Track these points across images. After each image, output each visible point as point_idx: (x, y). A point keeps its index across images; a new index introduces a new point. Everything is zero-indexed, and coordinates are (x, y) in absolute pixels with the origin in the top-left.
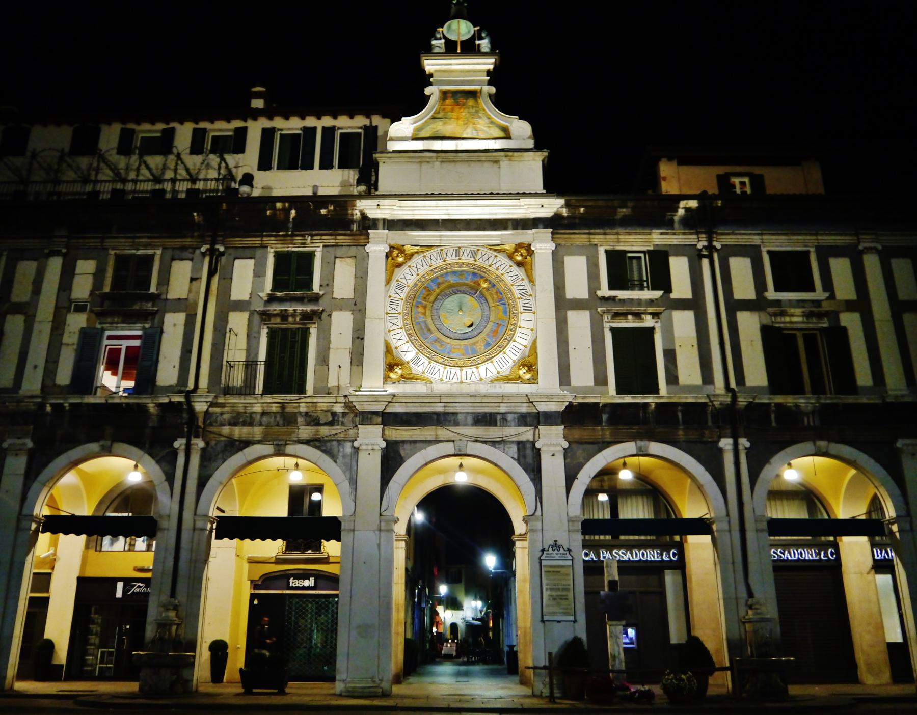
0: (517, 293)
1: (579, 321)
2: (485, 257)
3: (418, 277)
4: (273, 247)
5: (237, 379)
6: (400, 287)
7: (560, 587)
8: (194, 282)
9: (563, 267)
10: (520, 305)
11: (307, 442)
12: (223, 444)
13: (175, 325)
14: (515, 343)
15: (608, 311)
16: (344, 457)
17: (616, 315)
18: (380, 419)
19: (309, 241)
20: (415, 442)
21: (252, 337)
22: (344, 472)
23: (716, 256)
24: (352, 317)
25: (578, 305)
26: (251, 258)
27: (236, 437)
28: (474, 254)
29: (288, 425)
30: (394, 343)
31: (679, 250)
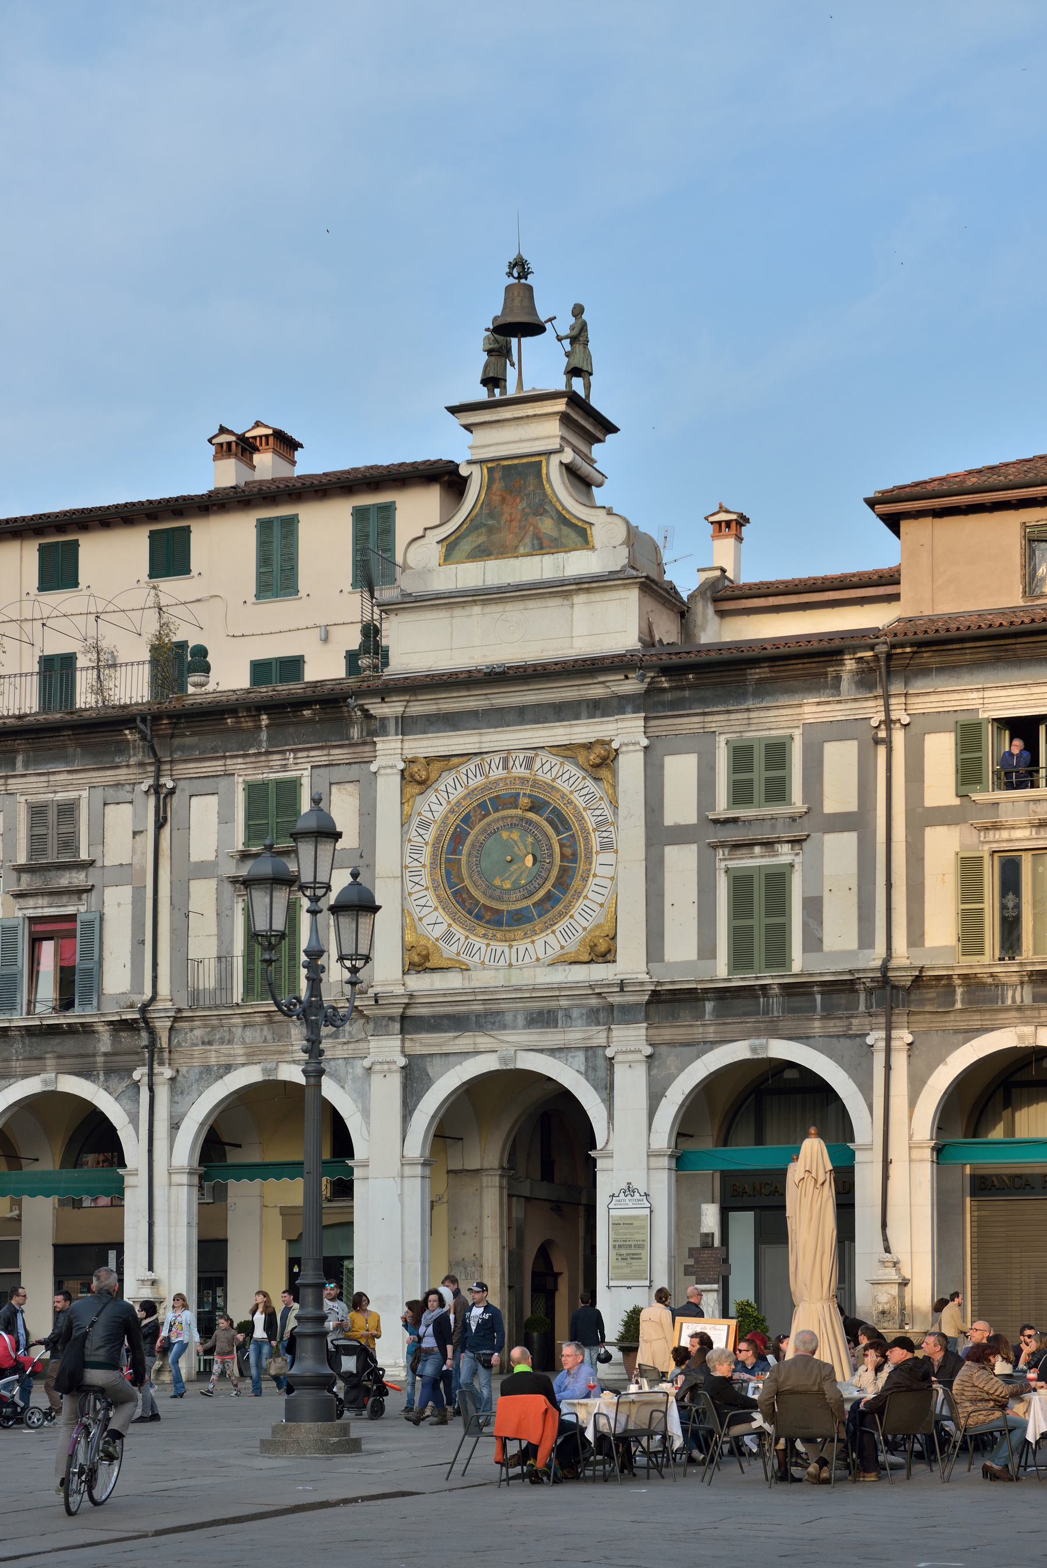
0: (590, 821)
1: (682, 862)
2: (547, 767)
4: (244, 773)
5: (208, 979)
6: (425, 825)
7: (633, 1243)
8: (137, 837)
9: (663, 775)
10: (595, 840)
14: (586, 902)
15: (722, 845)
16: (354, 1080)
18: (397, 1026)
19: (291, 761)
21: (223, 916)
22: (355, 1101)
25: (681, 835)
26: (213, 794)
27: (213, 1061)
28: (529, 763)
30: (417, 912)
31: (840, 731)
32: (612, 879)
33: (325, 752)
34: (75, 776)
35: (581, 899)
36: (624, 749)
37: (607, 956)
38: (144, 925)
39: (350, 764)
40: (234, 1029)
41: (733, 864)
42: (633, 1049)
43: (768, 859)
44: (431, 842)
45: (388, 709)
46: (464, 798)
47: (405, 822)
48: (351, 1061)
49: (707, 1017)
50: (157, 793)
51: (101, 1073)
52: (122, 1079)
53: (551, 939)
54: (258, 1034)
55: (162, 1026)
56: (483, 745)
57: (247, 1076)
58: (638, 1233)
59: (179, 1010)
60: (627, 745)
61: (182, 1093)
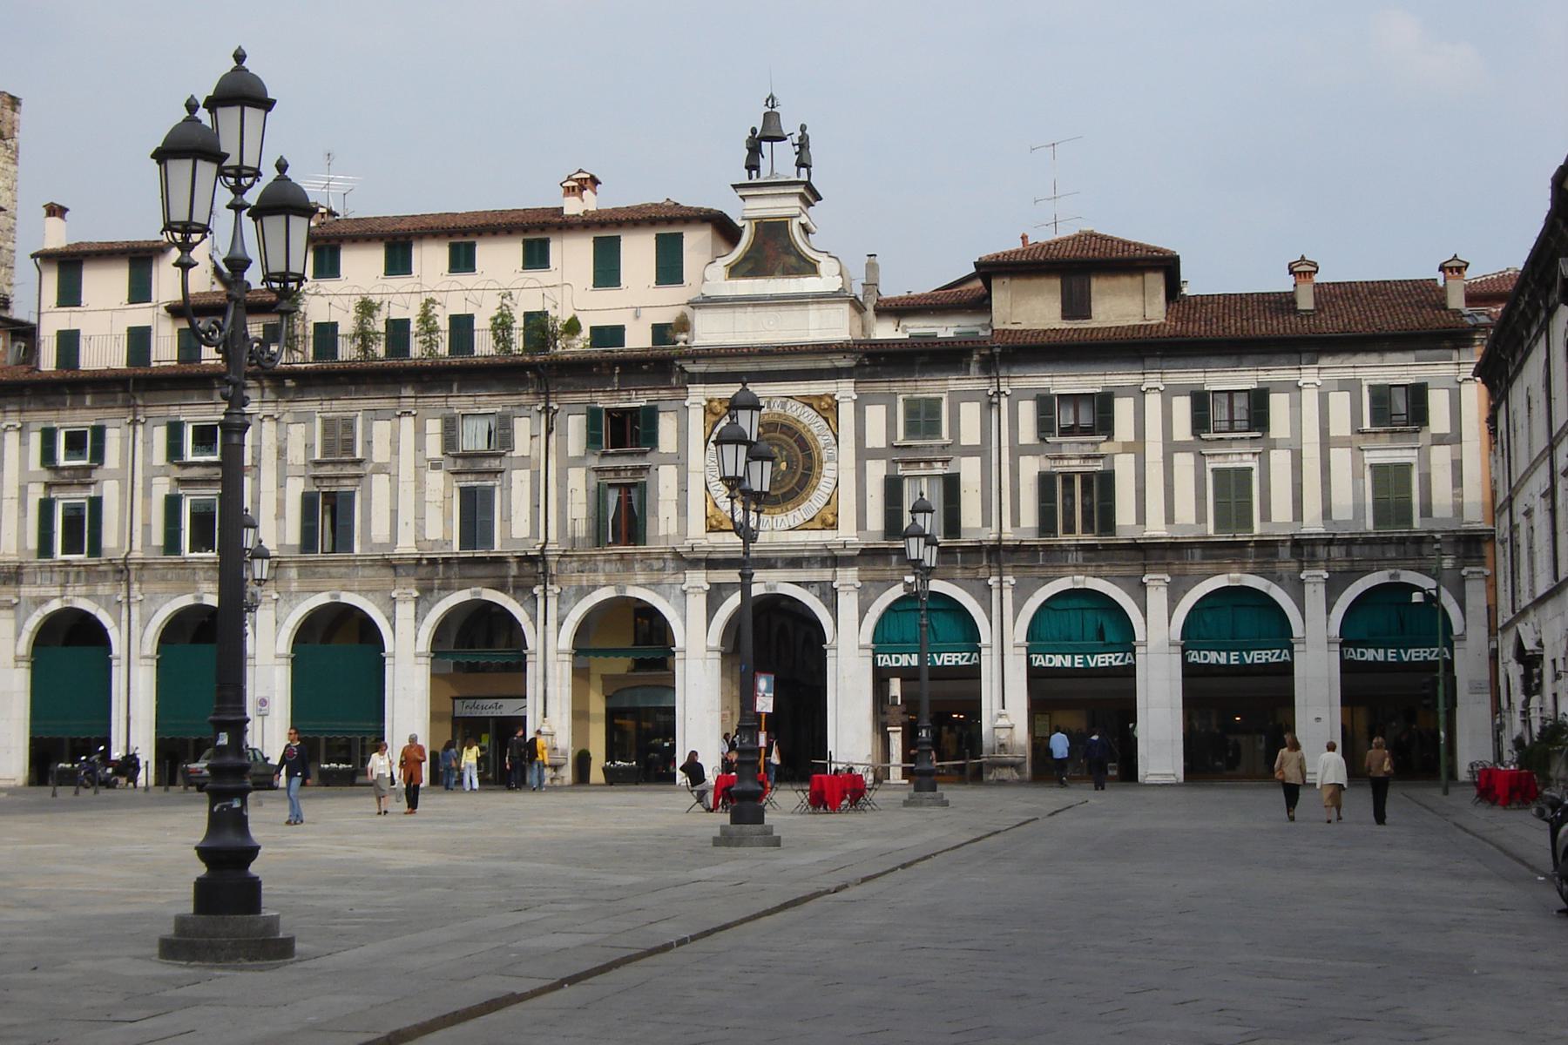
0: (822, 443)
11: (643, 586)
23: (1004, 402)
25: (875, 454)
28: (784, 405)
37: (833, 526)
45: (691, 368)
53: (797, 513)
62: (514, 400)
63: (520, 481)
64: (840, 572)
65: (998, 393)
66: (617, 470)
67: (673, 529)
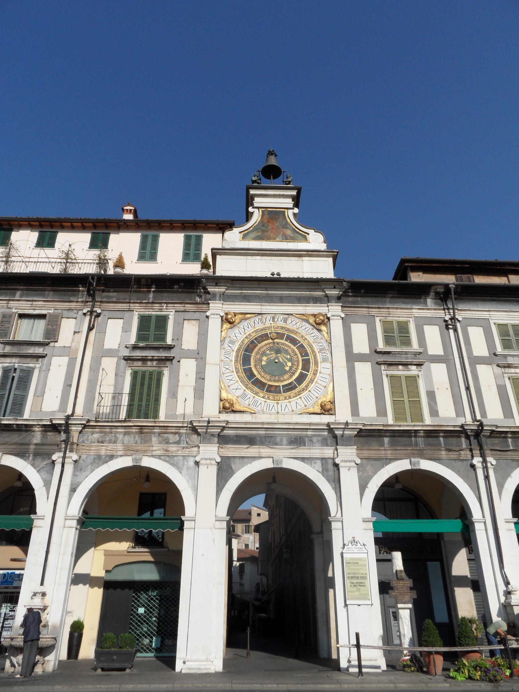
1: (364, 371)
2: (294, 323)
3: (245, 336)
7: (359, 576)
8: (76, 334)
9: (350, 331)
11: (159, 457)
12: (92, 457)
13: (60, 366)
16: (188, 468)
17: (390, 364)
18: (216, 439)
19: (165, 307)
20: (243, 457)
22: (188, 481)
23: (458, 325)
24: (196, 363)
25: (362, 358)
27: (103, 452)
28: (285, 321)
29: (144, 443)
31: (430, 321)
32: (329, 375)
33: (182, 305)
34: (47, 303)
35: (314, 383)
36: (332, 318)
38: (72, 377)
39: (195, 312)
40: (118, 435)
41: (390, 373)
42: (350, 460)
43: (406, 372)
44: (235, 350)
46: (253, 333)
47: (223, 341)
48: (187, 458)
49: (386, 446)
50: (91, 314)
51: (31, 455)
52: (44, 459)
53: (299, 401)
54: (132, 439)
55: (75, 430)
56: (263, 310)
57: (124, 462)
58: (362, 569)
59: (89, 421)
60: (334, 316)
61: (81, 470)
62: (66, 305)
63: (58, 366)
64: (342, 450)
65: (453, 319)
66: (144, 360)
67: (189, 410)
